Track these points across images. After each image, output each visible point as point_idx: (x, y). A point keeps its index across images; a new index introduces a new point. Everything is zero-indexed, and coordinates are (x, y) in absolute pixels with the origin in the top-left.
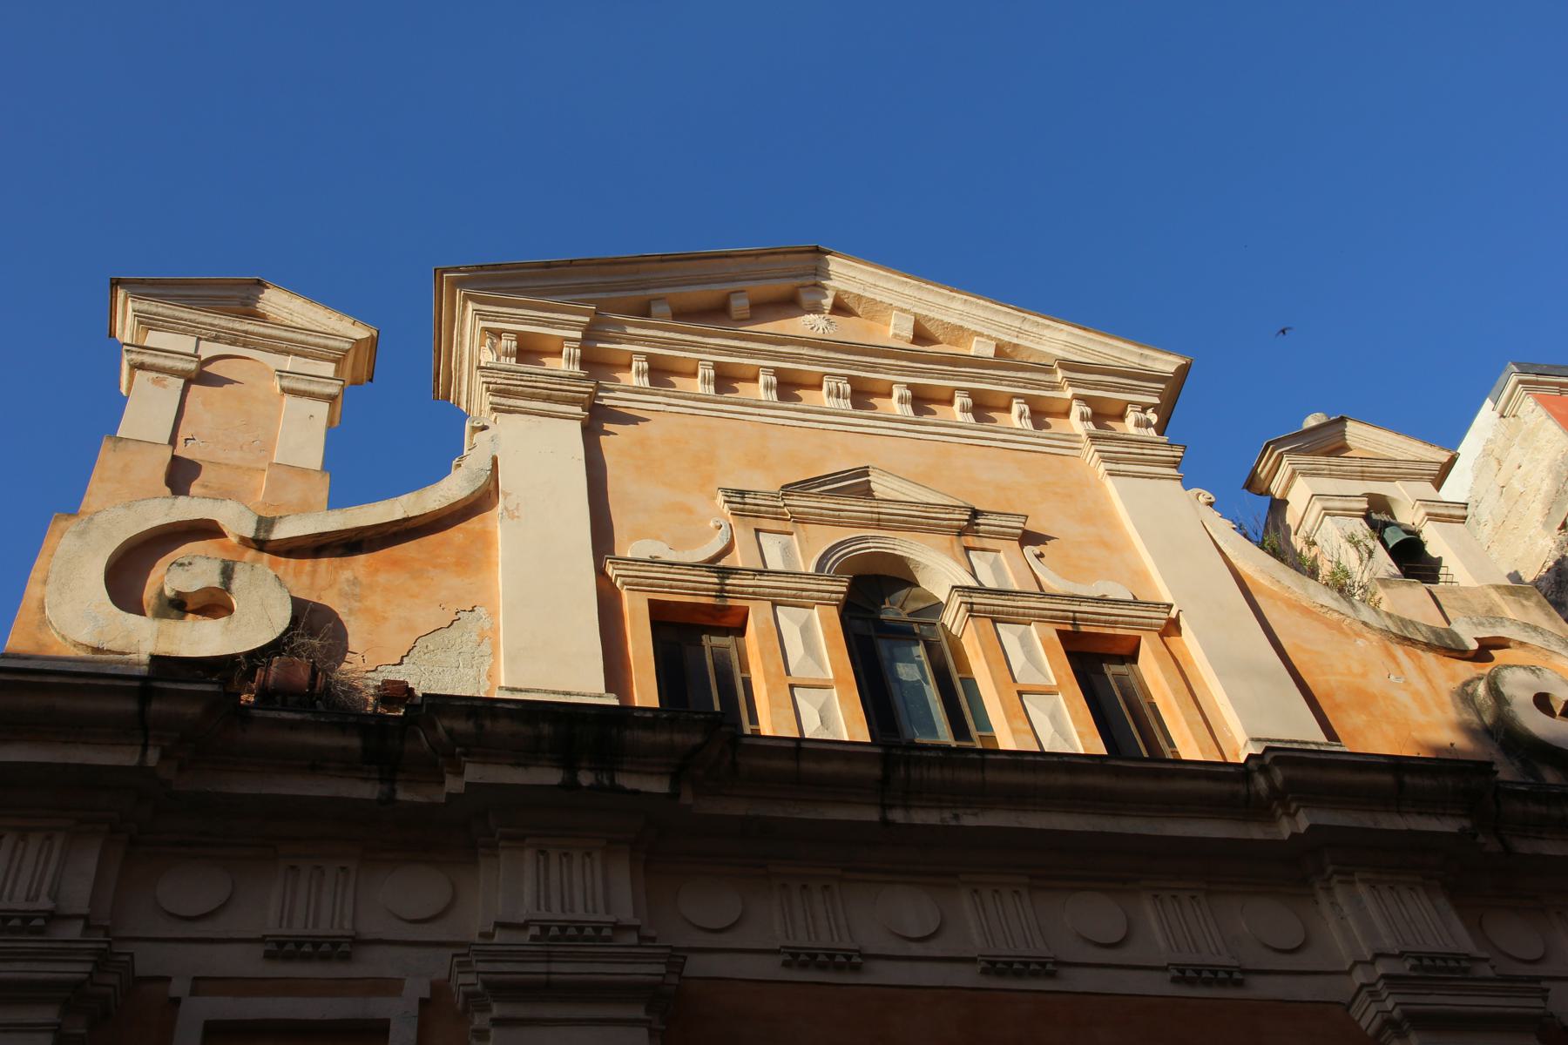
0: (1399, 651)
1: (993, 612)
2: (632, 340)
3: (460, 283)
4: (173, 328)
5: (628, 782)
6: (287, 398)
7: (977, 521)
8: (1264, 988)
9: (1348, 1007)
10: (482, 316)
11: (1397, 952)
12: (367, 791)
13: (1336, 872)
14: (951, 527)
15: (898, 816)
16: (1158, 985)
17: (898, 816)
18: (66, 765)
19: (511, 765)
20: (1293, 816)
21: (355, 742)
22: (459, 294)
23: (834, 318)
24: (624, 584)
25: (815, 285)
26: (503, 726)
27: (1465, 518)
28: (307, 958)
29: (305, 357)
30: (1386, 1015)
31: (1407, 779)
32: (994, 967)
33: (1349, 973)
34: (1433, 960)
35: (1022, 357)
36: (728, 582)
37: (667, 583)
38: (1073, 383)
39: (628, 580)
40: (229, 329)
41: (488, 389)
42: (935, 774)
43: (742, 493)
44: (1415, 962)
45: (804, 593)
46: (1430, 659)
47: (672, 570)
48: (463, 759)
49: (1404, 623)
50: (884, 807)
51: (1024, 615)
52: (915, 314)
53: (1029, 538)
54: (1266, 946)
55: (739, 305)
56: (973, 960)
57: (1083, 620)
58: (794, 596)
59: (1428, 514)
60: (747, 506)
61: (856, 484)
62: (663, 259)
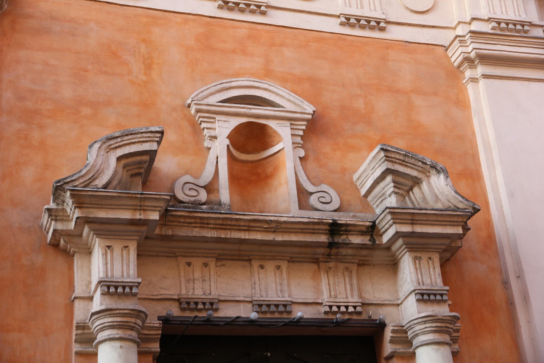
9: (447, 50)
11: (486, 18)
30: (466, 55)
33: (454, 28)
34: (515, 25)
44: (496, 25)
54: (407, 8)
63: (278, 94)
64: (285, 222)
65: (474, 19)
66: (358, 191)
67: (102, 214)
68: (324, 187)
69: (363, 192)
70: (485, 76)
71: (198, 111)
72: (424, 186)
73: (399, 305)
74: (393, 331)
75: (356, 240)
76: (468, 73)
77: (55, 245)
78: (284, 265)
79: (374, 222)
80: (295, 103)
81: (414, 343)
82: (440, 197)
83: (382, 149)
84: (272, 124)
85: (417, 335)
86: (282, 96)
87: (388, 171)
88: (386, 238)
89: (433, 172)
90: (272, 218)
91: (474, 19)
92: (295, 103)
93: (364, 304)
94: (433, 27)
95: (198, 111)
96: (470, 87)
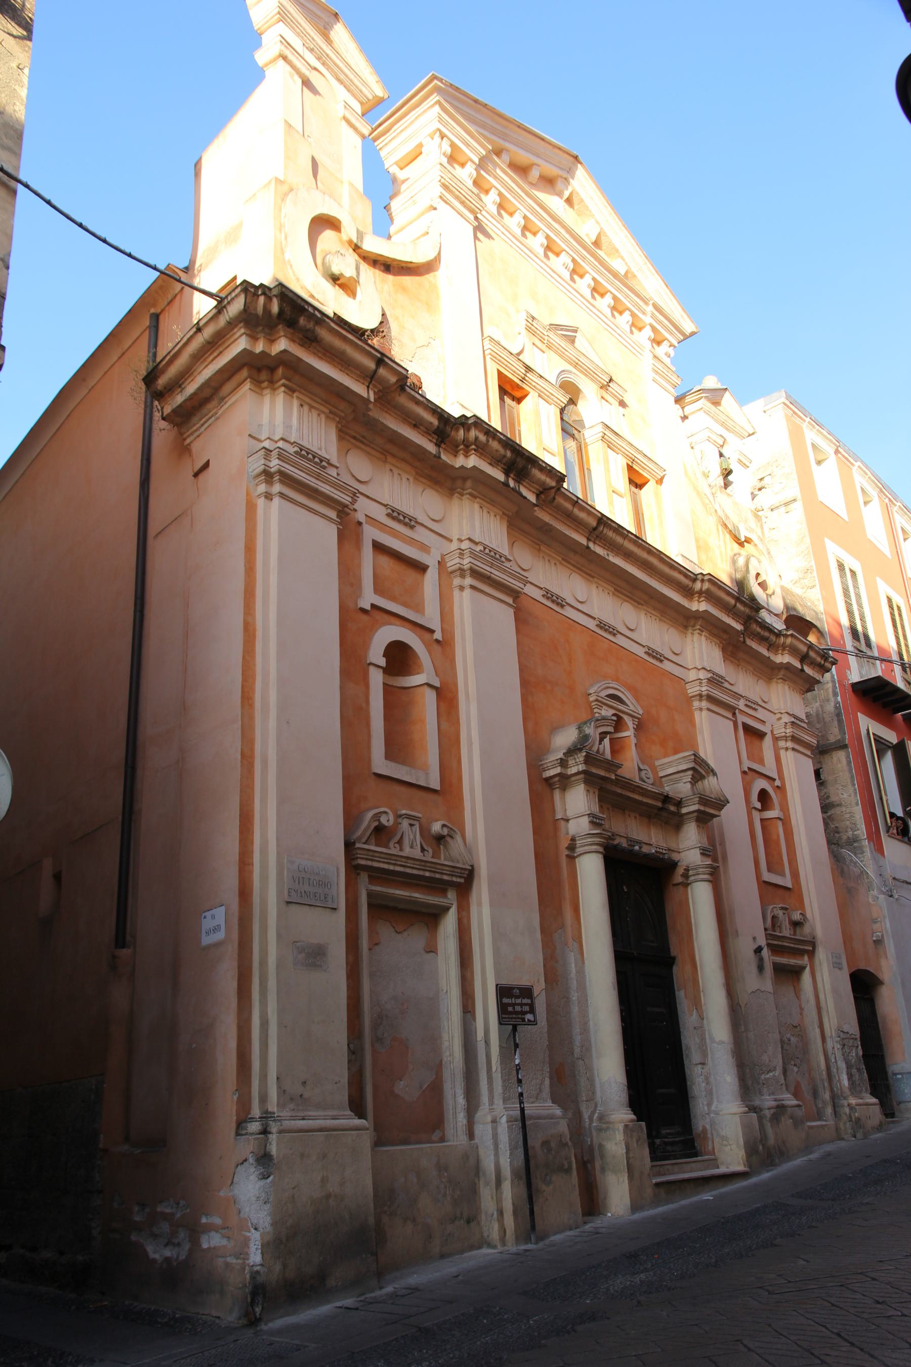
0: (720, 528)
1: (610, 442)
2: (495, 178)
3: (437, 89)
4: (294, 29)
5: (524, 492)
6: (344, 123)
7: (610, 384)
8: (667, 666)
10: (441, 120)
11: (709, 669)
12: (431, 448)
13: (699, 629)
14: (600, 382)
15: (591, 545)
16: (640, 652)
17: (591, 545)
18: (342, 384)
19: (489, 463)
20: (699, 602)
21: (436, 422)
22: (435, 98)
23: (565, 204)
24: (490, 354)
25: (566, 179)
27: (748, 467)
28: (399, 521)
29: (348, 91)
31: (738, 605)
32: (602, 625)
35: (632, 283)
36: (528, 375)
37: (506, 363)
38: (653, 316)
39: (493, 353)
40: (320, 47)
41: (440, 181)
42: (610, 534)
43: (533, 318)
45: (552, 397)
46: (728, 536)
47: (510, 357)
48: (473, 452)
49: (727, 517)
50: (589, 540)
51: (619, 449)
52: (601, 229)
53: (622, 404)
54: (671, 649)
55: (535, 174)
56: (594, 619)
57: (637, 463)
58: (548, 396)
59: (739, 459)
60: (532, 327)
61: (570, 334)
62: (520, 126)
63: (627, 698)
64: (649, 790)
66: (657, 773)
67: (594, 770)
68: (646, 767)
69: (661, 774)
70: (709, 710)
71: (597, 700)
72: (706, 782)
73: (679, 852)
74: (685, 869)
75: (672, 808)
76: (696, 704)
77: (547, 780)
78: (638, 817)
79: (681, 799)
80: (635, 706)
81: (692, 878)
82: (713, 790)
83: (694, 755)
84: (625, 717)
85: (698, 874)
86: (629, 699)
87: (693, 769)
88: (684, 810)
89: (711, 774)
90: (645, 787)
92: (635, 706)
93: (669, 850)
94: (681, 666)
95: (597, 700)
96: (697, 714)
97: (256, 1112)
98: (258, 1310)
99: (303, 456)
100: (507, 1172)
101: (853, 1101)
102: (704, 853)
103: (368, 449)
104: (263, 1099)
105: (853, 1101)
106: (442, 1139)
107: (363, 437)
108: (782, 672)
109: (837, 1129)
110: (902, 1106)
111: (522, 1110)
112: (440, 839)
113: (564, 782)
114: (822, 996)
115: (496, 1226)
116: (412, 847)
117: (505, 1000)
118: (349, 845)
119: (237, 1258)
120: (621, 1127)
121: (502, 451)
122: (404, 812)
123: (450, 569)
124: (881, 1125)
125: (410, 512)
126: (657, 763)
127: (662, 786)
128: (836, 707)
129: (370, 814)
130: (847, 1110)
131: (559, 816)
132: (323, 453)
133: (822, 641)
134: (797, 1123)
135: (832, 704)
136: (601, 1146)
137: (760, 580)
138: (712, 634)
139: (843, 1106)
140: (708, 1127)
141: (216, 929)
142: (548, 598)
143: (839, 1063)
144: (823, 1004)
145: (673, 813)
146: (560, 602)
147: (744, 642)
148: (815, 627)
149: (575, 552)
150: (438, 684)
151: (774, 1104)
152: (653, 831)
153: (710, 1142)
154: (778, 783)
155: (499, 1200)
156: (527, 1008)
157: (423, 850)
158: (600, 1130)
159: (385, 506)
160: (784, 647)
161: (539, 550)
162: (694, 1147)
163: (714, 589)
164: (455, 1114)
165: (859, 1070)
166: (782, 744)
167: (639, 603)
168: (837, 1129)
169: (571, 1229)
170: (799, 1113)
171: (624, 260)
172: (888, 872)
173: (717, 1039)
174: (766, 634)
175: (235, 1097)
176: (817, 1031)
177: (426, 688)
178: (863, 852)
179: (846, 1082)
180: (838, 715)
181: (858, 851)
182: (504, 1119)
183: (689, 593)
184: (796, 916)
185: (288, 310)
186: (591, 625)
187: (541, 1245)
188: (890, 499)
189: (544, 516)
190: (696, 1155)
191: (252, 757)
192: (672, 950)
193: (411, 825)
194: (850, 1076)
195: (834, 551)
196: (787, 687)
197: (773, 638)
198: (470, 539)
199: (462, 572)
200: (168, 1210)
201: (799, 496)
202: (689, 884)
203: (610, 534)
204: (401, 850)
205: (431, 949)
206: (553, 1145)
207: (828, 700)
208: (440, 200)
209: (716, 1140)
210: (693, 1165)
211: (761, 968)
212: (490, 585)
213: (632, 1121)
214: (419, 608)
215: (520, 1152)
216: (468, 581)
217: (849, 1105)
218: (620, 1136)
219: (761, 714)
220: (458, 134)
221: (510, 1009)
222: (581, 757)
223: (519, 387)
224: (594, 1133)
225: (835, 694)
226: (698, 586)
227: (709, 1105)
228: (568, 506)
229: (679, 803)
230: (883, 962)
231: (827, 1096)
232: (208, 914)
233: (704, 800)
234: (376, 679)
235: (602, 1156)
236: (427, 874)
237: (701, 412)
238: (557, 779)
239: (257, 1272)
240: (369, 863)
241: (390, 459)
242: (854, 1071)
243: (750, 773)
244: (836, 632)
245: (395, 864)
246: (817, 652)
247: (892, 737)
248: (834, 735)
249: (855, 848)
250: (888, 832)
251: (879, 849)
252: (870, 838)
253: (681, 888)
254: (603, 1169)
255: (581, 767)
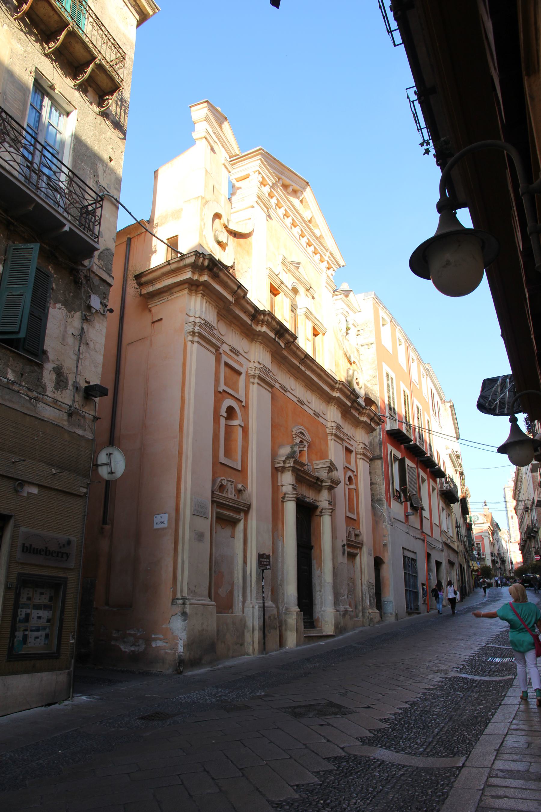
2: (277, 192)
3: (261, 154)
6: (223, 166)
10: (260, 167)
12: (249, 322)
15: (300, 366)
16: (311, 412)
17: (300, 366)
21: (253, 312)
26: (274, 323)
31: (351, 395)
38: (329, 257)
42: (308, 362)
43: (285, 258)
46: (346, 360)
49: (347, 351)
50: (300, 363)
53: (313, 298)
55: (290, 189)
62: (289, 170)
65: (334, 422)
67: (296, 466)
69: (315, 467)
70: (335, 440)
71: (295, 434)
72: (333, 473)
75: (319, 483)
76: (329, 437)
77: (276, 468)
81: (323, 513)
87: (329, 467)
88: (324, 484)
91: (334, 422)
93: (316, 501)
96: (329, 441)
97: (179, 595)
98: (181, 669)
99: (206, 325)
100: (257, 627)
101: (370, 611)
102: (330, 503)
103: (225, 320)
104: (182, 591)
105: (370, 611)
106: (232, 613)
107: (225, 315)
108: (362, 424)
109: (363, 622)
110: (386, 615)
111: (264, 603)
112: (240, 491)
113: (283, 469)
114: (363, 567)
115: (251, 648)
116: (231, 494)
117: (261, 560)
118: (213, 492)
119: (171, 650)
120: (295, 613)
121: (276, 326)
122: (229, 479)
123: (249, 374)
124: (379, 621)
125: (238, 349)
126: (314, 462)
127: (315, 473)
128: (379, 440)
129: (219, 479)
130: (368, 614)
131: (279, 484)
132: (212, 324)
133: (377, 410)
134: (351, 618)
135: (378, 439)
136: (286, 621)
137: (357, 381)
138: (339, 406)
139: (366, 613)
140: (320, 617)
141: (164, 522)
142: (281, 388)
143: (366, 595)
144: (363, 570)
145: (319, 485)
146: (285, 389)
147: (350, 410)
148: (375, 403)
149: (293, 368)
150: (243, 425)
151: (344, 609)
152: (311, 492)
153: (320, 623)
154: (355, 473)
155: (253, 637)
156: (268, 563)
157: (234, 495)
158: (286, 614)
159: (229, 346)
160: (365, 414)
161: (280, 366)
162: (313, 625)
163: (343, 388)
164: (238, 603)
165: (373, 598)
166: (358, 456)
167: (313, 391)
168: (363, 622)
169: (276, 651)
170: (352, 614)
171: (320, 230)
172: (392, 515)
173: (327, 581)
174: (359, 408)
175: (172, 590)
176: (360, 581)
177: (239, 426)
178: (383, 506)
179: (368, 603)
180: (380, 444)
181: (381, 505)
182: (257, 607)
183: (333, 388)
184: (357, 532)
185: (211, 264)
186: (295, 400)
187: (267, 656)
188: (409, 345)
189: (285, 353)
190: (314, 627)
191: (182, 453)
192: (312, 543)
193: (231, 485)
194: (370, 601)
195: (386, 368)
196: (363, 431)
197: (361, 409)
198: (258, 362)
199: (254, 377)
200: (133, 632)
201: (375, 342)
202: (321, 516)
203: (308, 362)
204: (227, 495)
205: (233, 536)
206: (272, 618)
207: (376, 437)
208: (256, 203)
209: (323, 622)
210: (314, 631)
211: (344, 553)
212: (264, 383)
213: (299, 611)
214: (237, 391)
215: (262, 619)
216: (256, 381)
217: (369, 612)
218: (294, 617)
219: (352, 442)
220: (265, 172)
221: (262, 563)
222: (292, 460)
223: (277, 290)
224: (283, 616)
225: (380, 435)
226: (337, 386)
227: (321, 608)
228: (295, 349)
229: (322, 481)
230: (386, 554)
231: (361, 608)
232: (158, 516)
233: (332, 481)
234: (223, 421)
235: (286, 624)
236: (236, 506)
237: (341, 300)
238: (281, 468)
239: (181, 655)
240: (218, 500)
241: (233, 325)
242: (372, 599)
243: (346, 469)
244: (383, 407)
245: (226, 501)
246: (377, 417)
247: (399, 455)
248: (377, 452)
249: (380, 503)
250: (393, 497)
251: (389, 505)
252: (387, 500)
253: (319, 517)
254: (286, 630)
255: (292, 465)
